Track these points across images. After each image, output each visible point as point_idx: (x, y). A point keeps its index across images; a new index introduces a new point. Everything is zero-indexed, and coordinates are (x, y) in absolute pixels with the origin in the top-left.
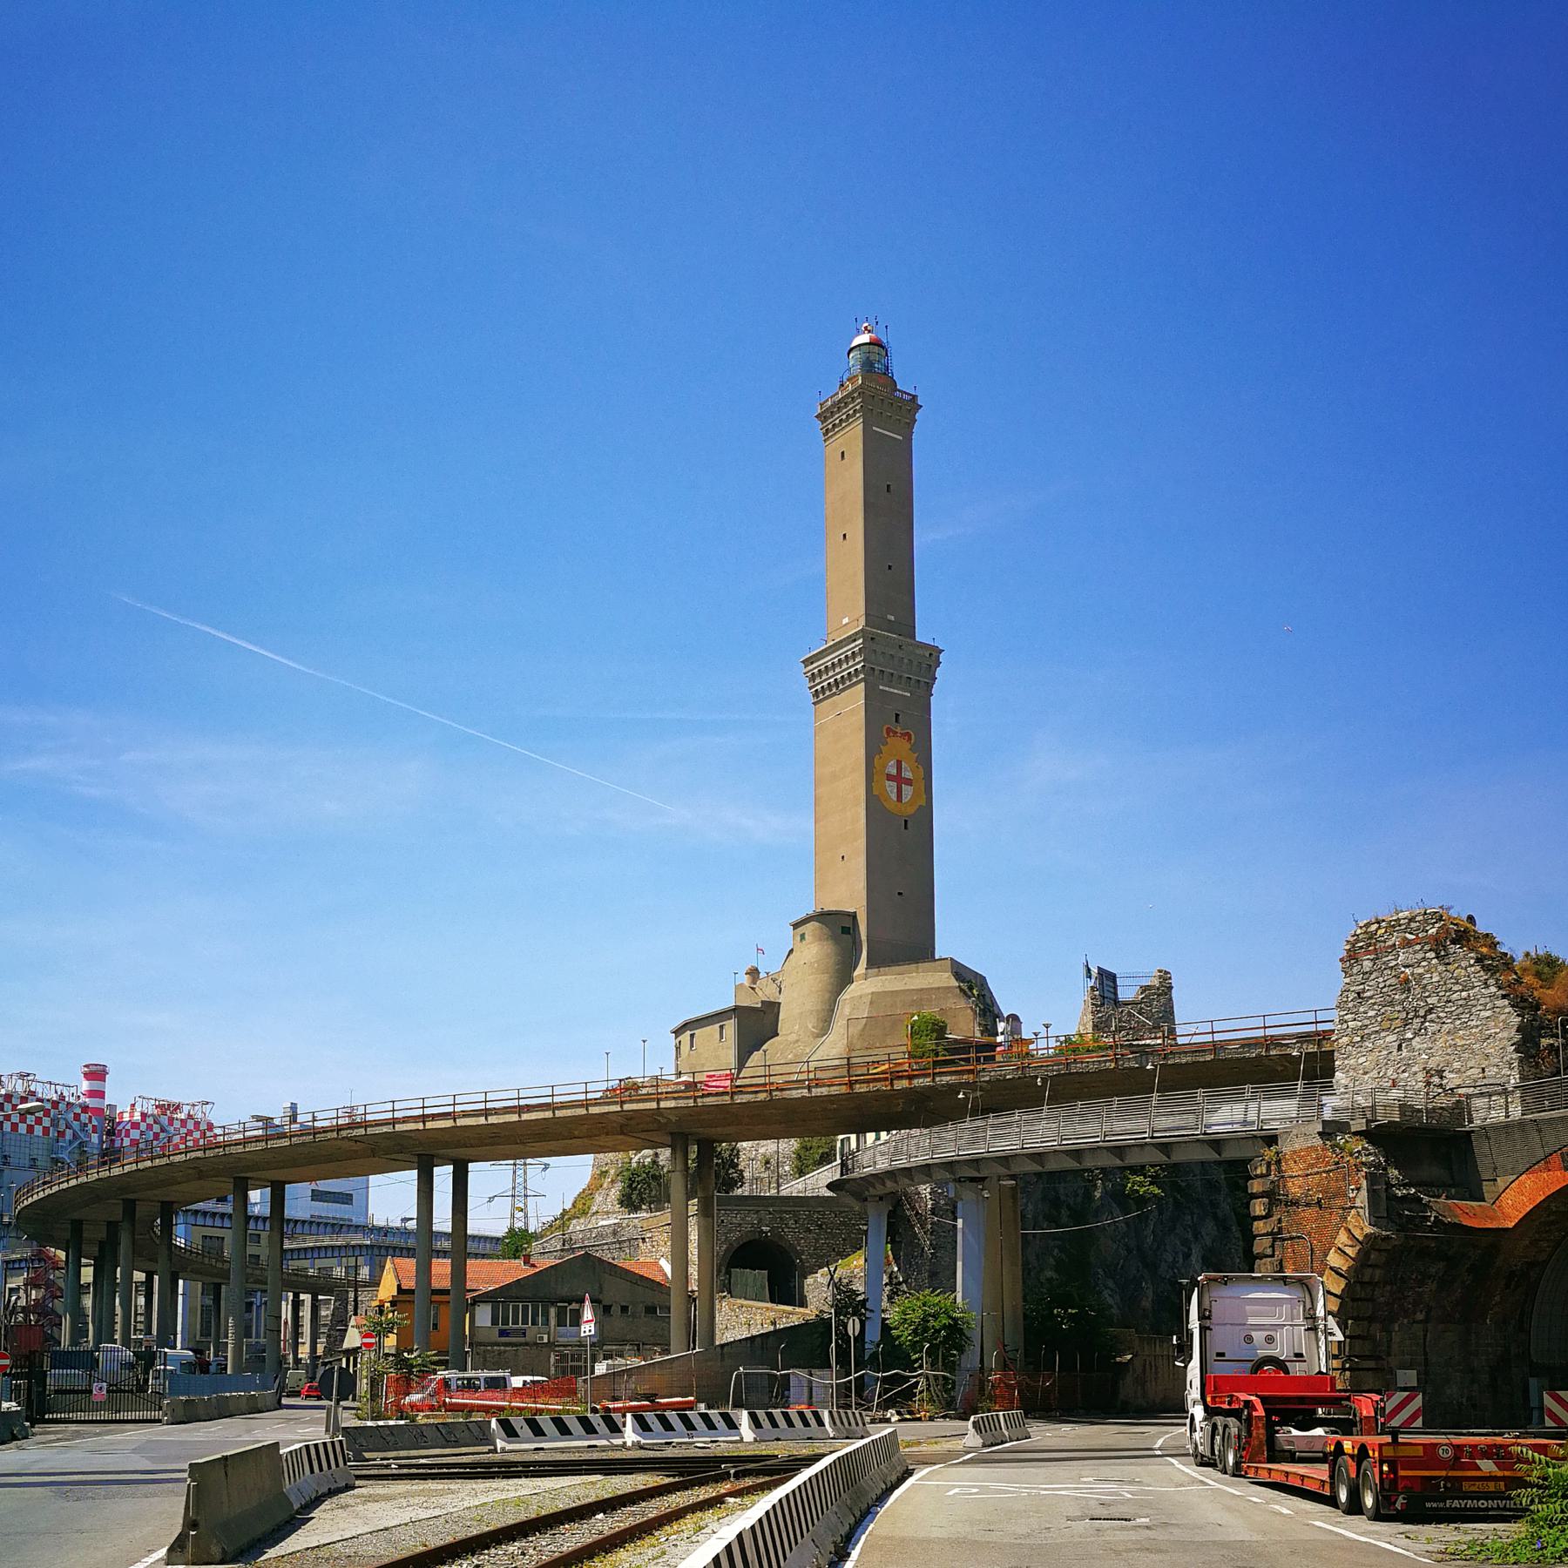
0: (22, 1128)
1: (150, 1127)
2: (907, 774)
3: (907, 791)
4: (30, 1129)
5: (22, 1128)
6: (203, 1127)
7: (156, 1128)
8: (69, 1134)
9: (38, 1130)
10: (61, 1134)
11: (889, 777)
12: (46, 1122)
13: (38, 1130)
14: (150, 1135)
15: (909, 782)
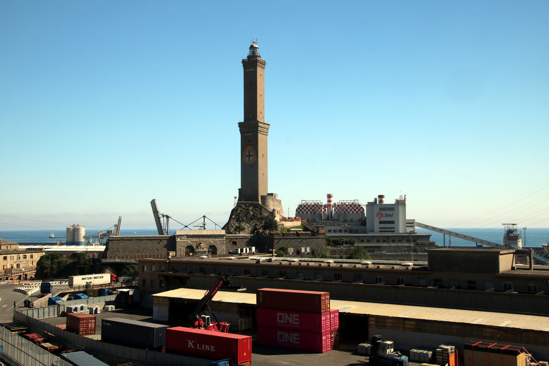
0: (305, 213)
1: (340, 208)
2: (251, 154)
3: (251, 158)
4: (307, 213)
5: (305, 213)
6: (357, 206)
7: (342, 208)
8: (317, 213)
9: (309, 213)
10: (315, 213)
11: (247, 156)
12: (311, 210)
13: (309, 213)
14: (341, 210)
15: (252, 156)
